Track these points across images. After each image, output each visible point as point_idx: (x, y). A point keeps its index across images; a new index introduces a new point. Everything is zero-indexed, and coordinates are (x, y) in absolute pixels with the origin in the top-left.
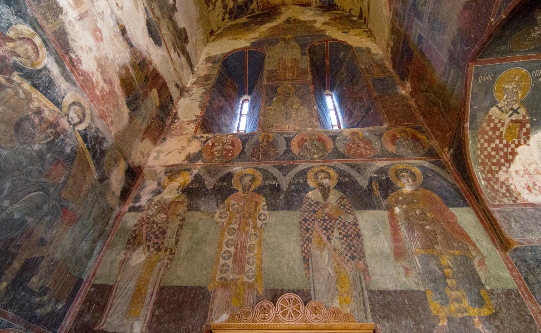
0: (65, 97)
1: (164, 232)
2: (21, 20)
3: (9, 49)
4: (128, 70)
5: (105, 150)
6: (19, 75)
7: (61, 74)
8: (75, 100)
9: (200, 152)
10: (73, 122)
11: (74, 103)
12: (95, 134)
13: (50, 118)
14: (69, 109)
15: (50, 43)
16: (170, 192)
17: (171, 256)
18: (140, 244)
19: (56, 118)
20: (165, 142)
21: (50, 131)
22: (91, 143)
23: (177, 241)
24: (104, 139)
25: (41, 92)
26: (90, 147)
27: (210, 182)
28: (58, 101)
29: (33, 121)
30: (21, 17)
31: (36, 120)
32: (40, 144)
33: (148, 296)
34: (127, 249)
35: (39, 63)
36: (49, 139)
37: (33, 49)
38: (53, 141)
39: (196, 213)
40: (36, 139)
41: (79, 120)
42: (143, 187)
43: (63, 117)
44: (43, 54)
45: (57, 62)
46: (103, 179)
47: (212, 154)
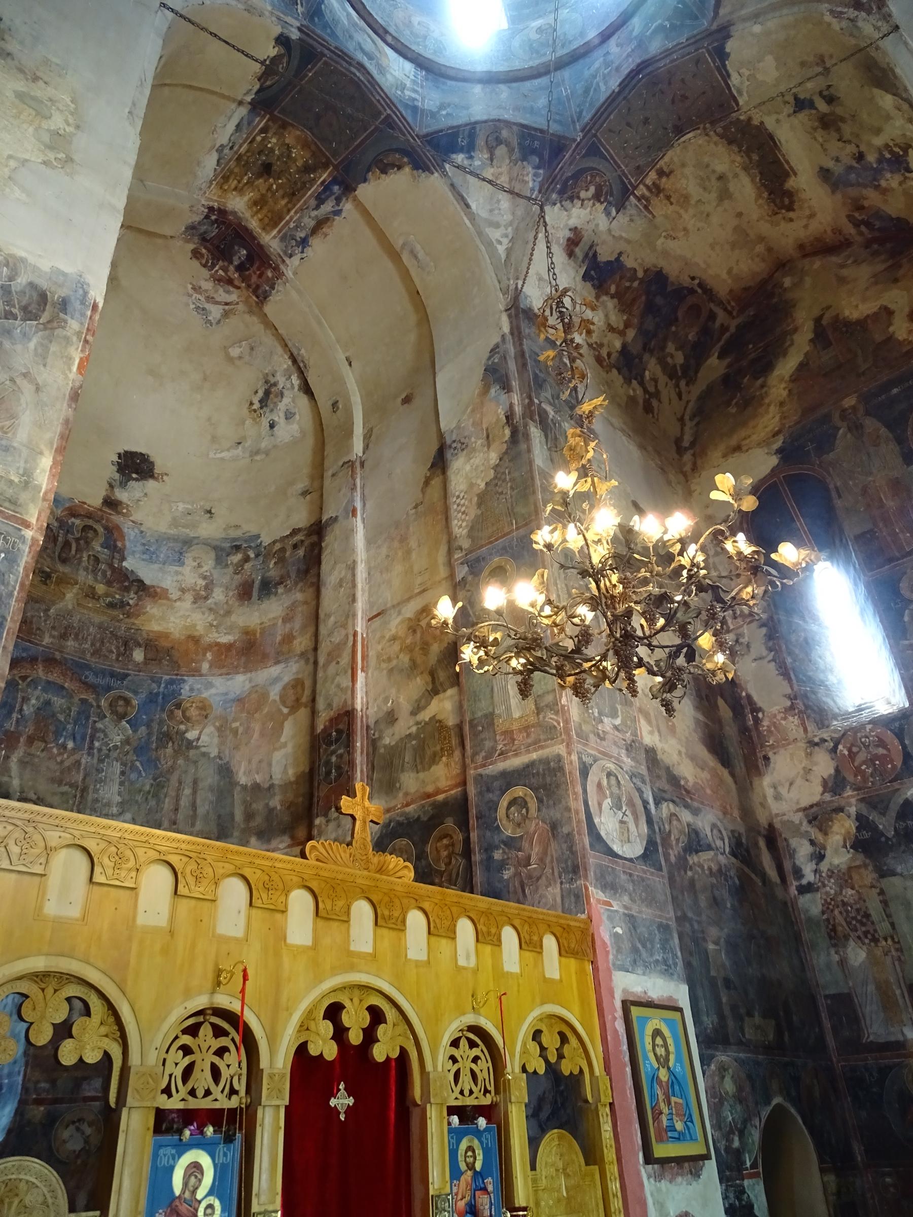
1: (867, 916)
9: (837, 770)
16: (836, 851)
17: (897, 946)
18: (846, 937)
20: (772, 765)
23: (893, 925)
27: (886, 824)
33: (901, 1001)
34: (835, 946)
39: (895, 880)
42: (792, 854)
47: (858, 771)
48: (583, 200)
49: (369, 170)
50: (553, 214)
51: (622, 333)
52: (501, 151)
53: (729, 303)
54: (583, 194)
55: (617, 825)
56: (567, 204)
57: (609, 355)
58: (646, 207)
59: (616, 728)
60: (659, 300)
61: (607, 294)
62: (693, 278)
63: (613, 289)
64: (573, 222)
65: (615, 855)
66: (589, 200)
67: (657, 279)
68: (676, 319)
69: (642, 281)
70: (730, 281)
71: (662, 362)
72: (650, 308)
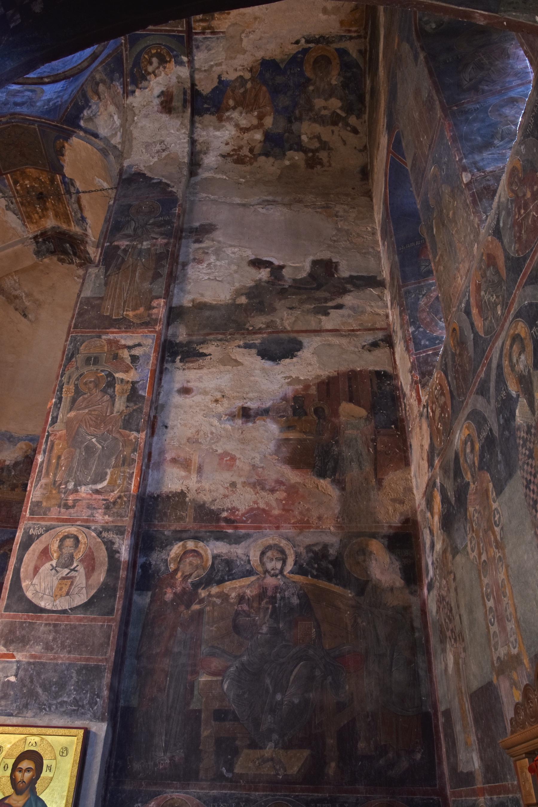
0: (251, 558)
2: (168, 548)
3: (180, 579)
4: (287, 440)
5: (337, 557)
6: (204, 589)
7: (230, 544)
8: (262, 549)
10: (277, 572)
11: (263, 554)
12: (311, 554)
13: (255, 592)
14: (262, 563)
15: (199, 532)
19: (260, 586)
21: (263, 603)
22: (313, 568)
24: (325, 547)
25: (229, 580)
26: (315, 573)
28: (248, 570)
29: (244, 611)
30: (166, 546)
31: (245, 607)
32: (265, 623)
35: (207, 560)
36: (270, 611)
37: (193, 556)
38: (274, 608)
40: (258, 623)
41: (281, 562)
43: (265, 578)
44: (203, 549)
45: (217, 539)
46: (363, 586)
48: (154, 72)
49: (59, 160)
50: (138, 99)
51: (259, 126)
52: (101, 87)
53: (349, 31)
54: (150, 69)
55: (56, 582)
56: (144, 84)
57: (251, 150)
58: (213, 33)
59: (97, 492)
60: (280, 79)
61: (227, 110)
62: (297, 42)
63: (231, 103)
64: (157, 91)
65: (43, 610)
66: (158, 68)
67: (267, 67)
68: (308, 80)
69: (252, 79)
70: (333, 17)
71: (321, 120)
72: (275, 91)
